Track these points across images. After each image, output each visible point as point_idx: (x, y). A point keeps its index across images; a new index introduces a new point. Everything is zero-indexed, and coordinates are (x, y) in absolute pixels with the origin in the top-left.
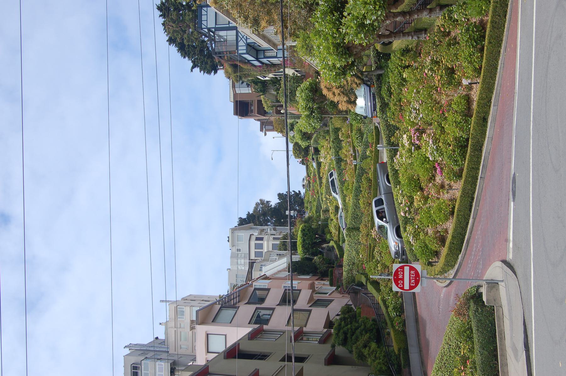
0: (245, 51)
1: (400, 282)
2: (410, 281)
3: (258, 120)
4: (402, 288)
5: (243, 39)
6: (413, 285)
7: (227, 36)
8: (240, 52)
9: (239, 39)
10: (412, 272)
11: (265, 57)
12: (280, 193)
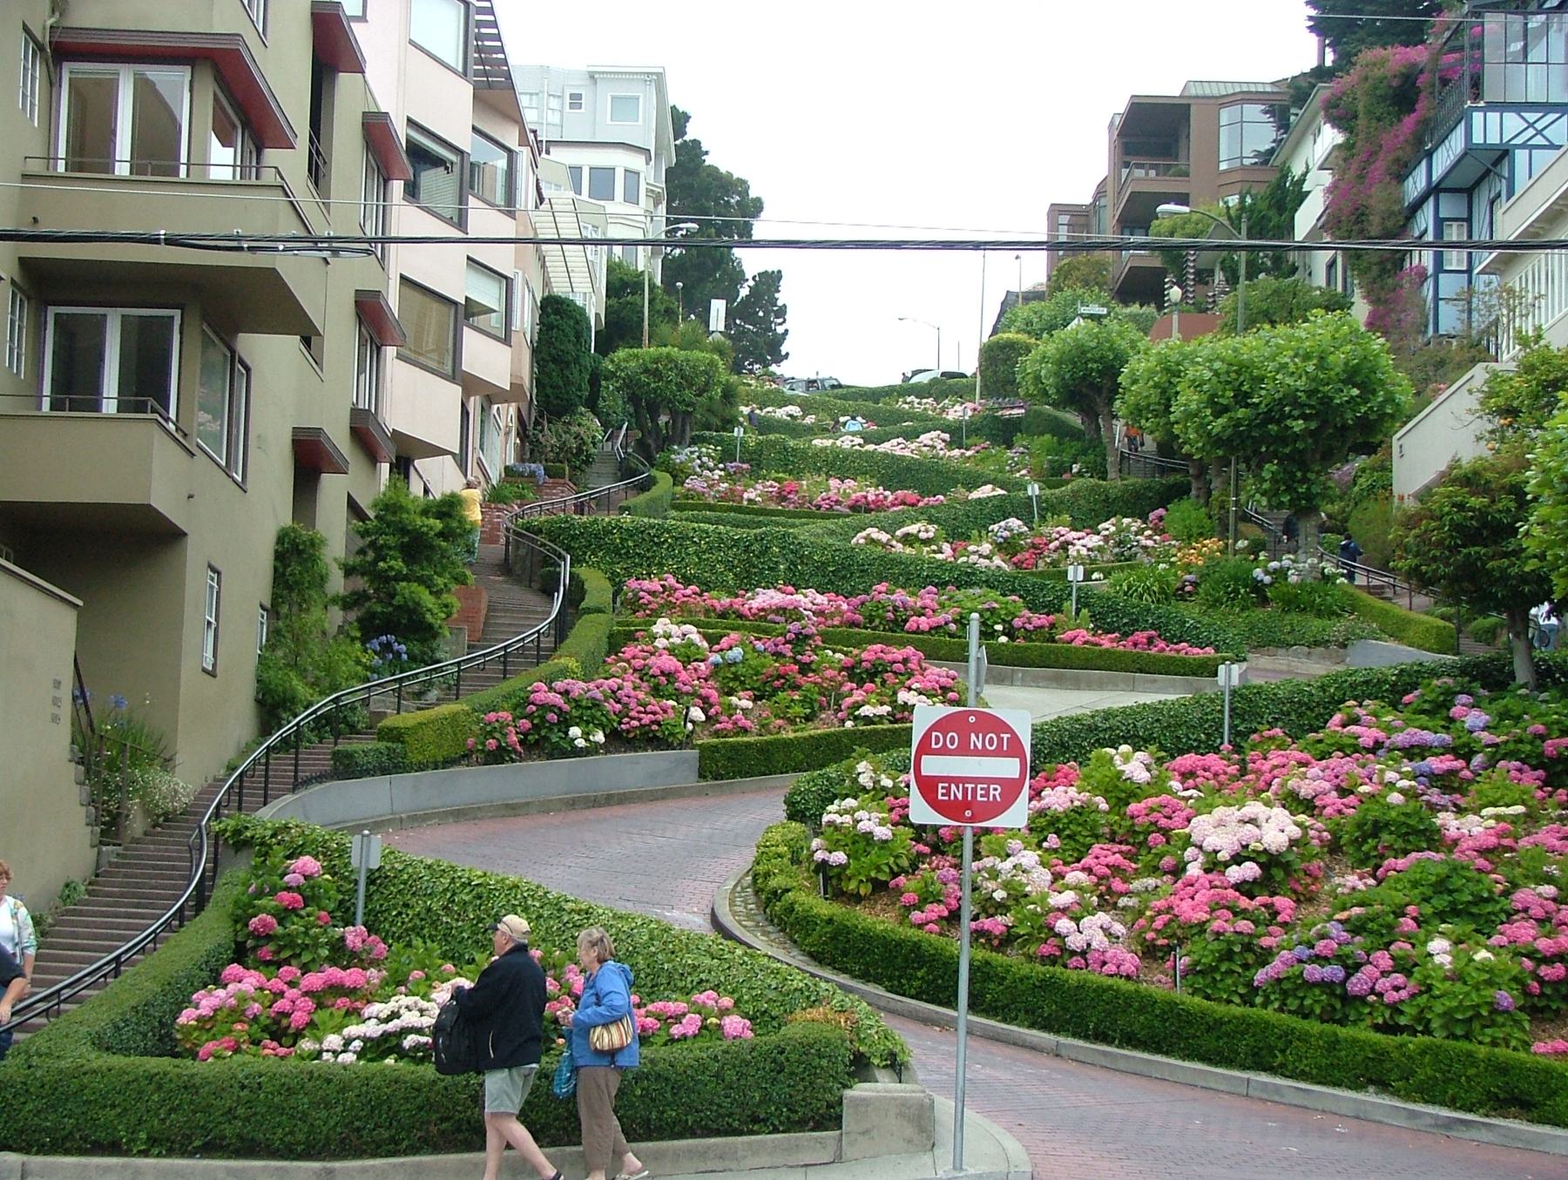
0: (1478, 138)
1: (952, 737)
2: (957, 780)
3: (1100, 192)
4: (925, 748)
5: (1531, 132)
6: (940, 791)
7: (1547, 63)
8: (1477, 117)
9: (1531, 117)
10: (995, 789)
11: (1440, 223)
12: (780, 278)
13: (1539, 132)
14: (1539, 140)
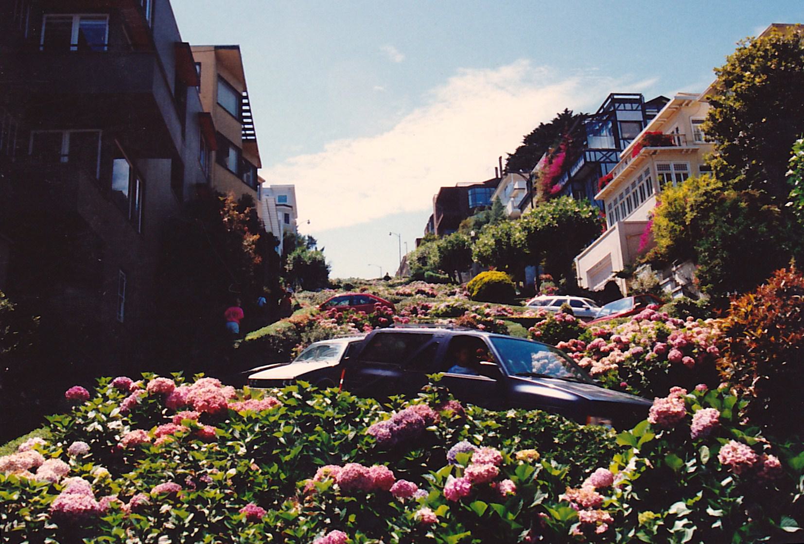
0: (588, 160)
8: (587, 153)
9: (604, 153)
13: (608, 158)
14: (608, 160)
